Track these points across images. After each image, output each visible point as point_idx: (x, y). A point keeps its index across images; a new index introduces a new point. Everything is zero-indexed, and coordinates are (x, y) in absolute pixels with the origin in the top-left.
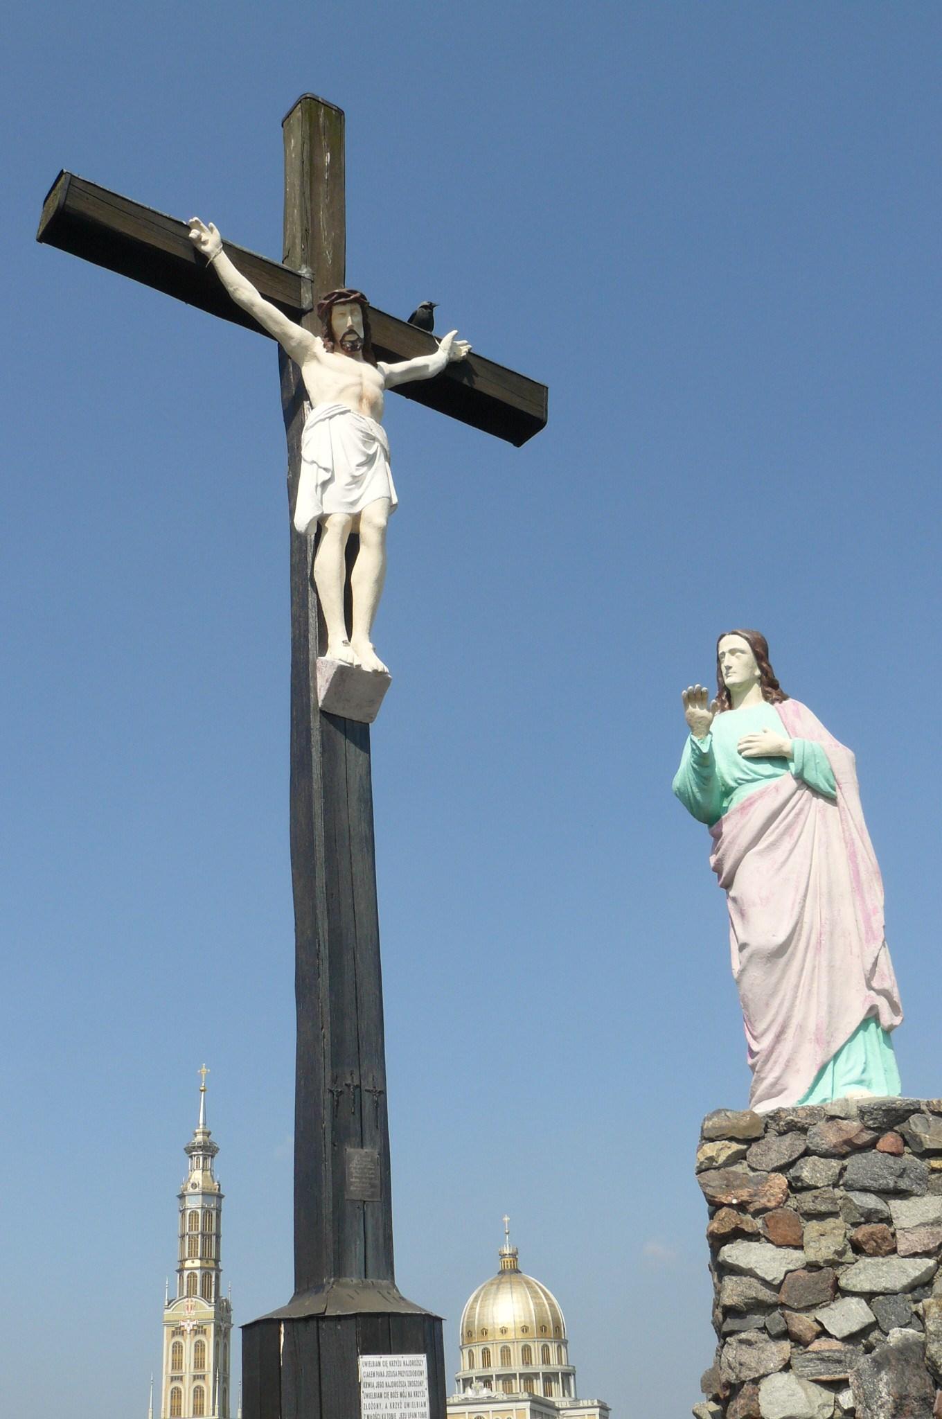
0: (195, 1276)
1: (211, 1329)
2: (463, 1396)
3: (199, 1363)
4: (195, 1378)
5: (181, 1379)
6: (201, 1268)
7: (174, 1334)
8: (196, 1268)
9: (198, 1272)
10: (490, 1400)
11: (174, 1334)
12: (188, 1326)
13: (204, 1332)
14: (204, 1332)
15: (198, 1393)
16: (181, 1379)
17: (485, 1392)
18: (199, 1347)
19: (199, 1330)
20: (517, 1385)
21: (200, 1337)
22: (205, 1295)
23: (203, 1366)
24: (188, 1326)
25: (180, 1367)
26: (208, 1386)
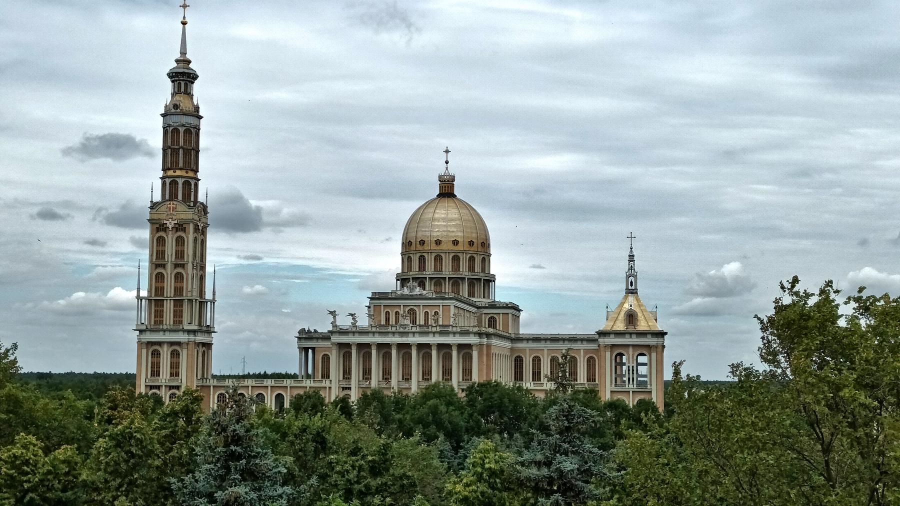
0: (177, 183)
2: (399, 293)
4: (176, 266)
5: (163, 266)
10: (421, 297)
11: (158, 230)
12: (170, 224)
13: (184, 230)
14: (184, 230)
15: (179, 277)
16: (163, 266)
17: (418, 291)
18: (180, 241)
19: (180, 227)
20: (447, 288)
21: (180, 234)
24: (170, 224)
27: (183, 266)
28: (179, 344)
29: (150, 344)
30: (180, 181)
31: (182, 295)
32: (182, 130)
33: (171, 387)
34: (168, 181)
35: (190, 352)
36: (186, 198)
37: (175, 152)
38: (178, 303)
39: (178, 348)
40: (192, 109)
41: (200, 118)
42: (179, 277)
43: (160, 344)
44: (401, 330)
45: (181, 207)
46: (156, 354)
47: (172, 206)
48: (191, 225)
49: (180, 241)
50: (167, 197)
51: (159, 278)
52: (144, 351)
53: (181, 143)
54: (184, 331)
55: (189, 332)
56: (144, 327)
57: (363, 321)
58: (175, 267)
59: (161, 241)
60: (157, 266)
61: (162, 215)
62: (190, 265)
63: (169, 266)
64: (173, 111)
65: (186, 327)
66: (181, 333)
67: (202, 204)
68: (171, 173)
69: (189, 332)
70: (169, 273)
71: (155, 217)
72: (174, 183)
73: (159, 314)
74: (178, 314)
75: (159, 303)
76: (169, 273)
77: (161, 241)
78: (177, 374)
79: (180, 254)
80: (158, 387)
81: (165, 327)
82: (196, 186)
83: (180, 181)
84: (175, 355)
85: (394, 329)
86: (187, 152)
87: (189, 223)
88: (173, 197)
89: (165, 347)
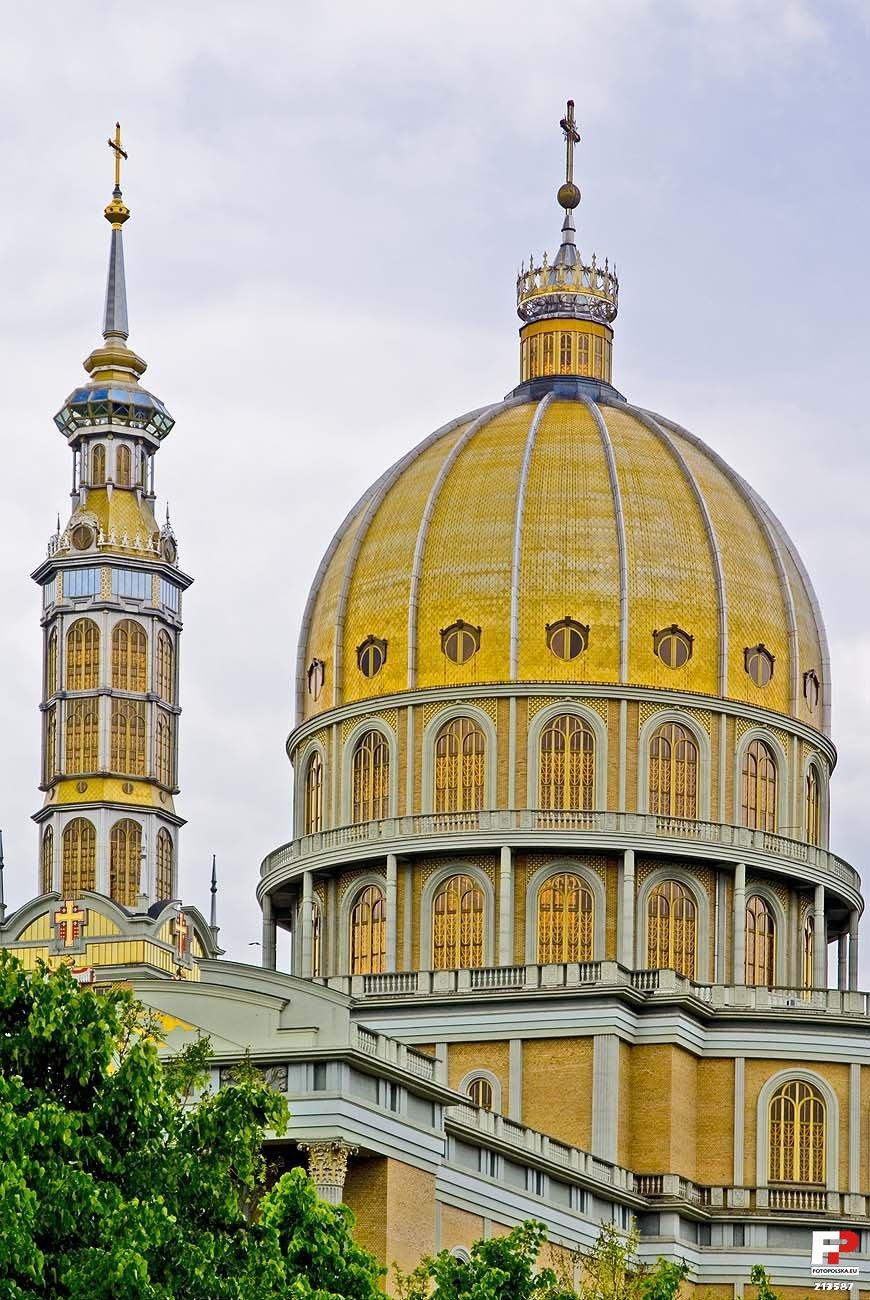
30: (103, 823)
32: (106, 623)
34: (59, 823)
36: (123, 879)
37: (84, 711)
40: (142, 545)
41: (182, 583)
45: (101, 923)
47: (70, 917)
50: (57, 886)
53: (105, 678)
64: (73, 552)
67: (191, 912)
68: (67, 793)
72: (80, 832)
82: (167, 843)
83: (103, 823)
86: (128, 715)
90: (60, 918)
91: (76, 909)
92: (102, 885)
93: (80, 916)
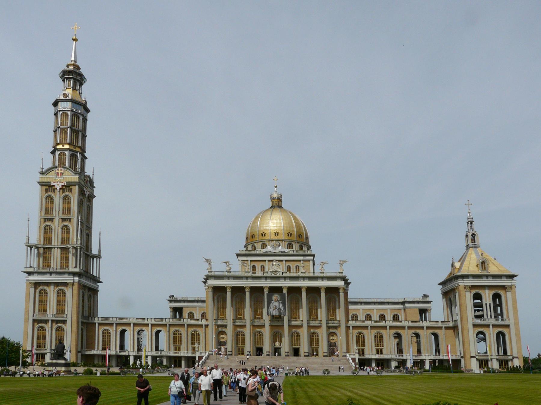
1: (76, 189)
3: (66, 211)
4: (63, 220)
5: (52, 220)
6: (69, 150)
7: (47, 191)
8: (66, 150)
9: (67, 153)
12: (58, 186)
13: (71, 191)
15: (65, 230)
16: (52, 220)
18: (66, 200)
22: (73, 166)
23: (69, 213)
24: (58, 186)
25: (52, 212)
26: (74, 226)
27: (69, 220)
28: (65, 284)
29: (37, 284)
31: (69, 243)
33: (57, 322)
35: (75, 292)
38: (65, 250)
39: (64, 288)
42: (65, 230)
43: (48, 284)
44: (273, 275)
46: (44, 293)
47: (60, 171)
48: (77, 187)
49: (66, 200)
50: (57, 165)
51: (48, 230)
52: (32, 290)
54: (70, 273)
55: (74, 274)
56: (31, 270)
57: (237, 268)
58: (62, 221)
59: (49, 200)
60: (46, 220)
61: (50, 178)
62: (75, 221)
63: (56, 220)
65: (71, 270)
66: (67, 275)
69: (74, 274)
70: (56, 226)
71: (45, 179)
73: (47, 261)
74: (64, 261)
75: (48, 250)
76: (56, 226)
77: (49, 200)
78: (64, 311)
79: (66, 211)
80: (46, 322)
81: (52, 270)
84: (61, 294)
85: (266, 275)
87: (74, 185)
88: (62, 164)
89: (52, 287)
90: (57, 171)
91: (61, 170)
92: (67, 165)
93: (62, 171)
